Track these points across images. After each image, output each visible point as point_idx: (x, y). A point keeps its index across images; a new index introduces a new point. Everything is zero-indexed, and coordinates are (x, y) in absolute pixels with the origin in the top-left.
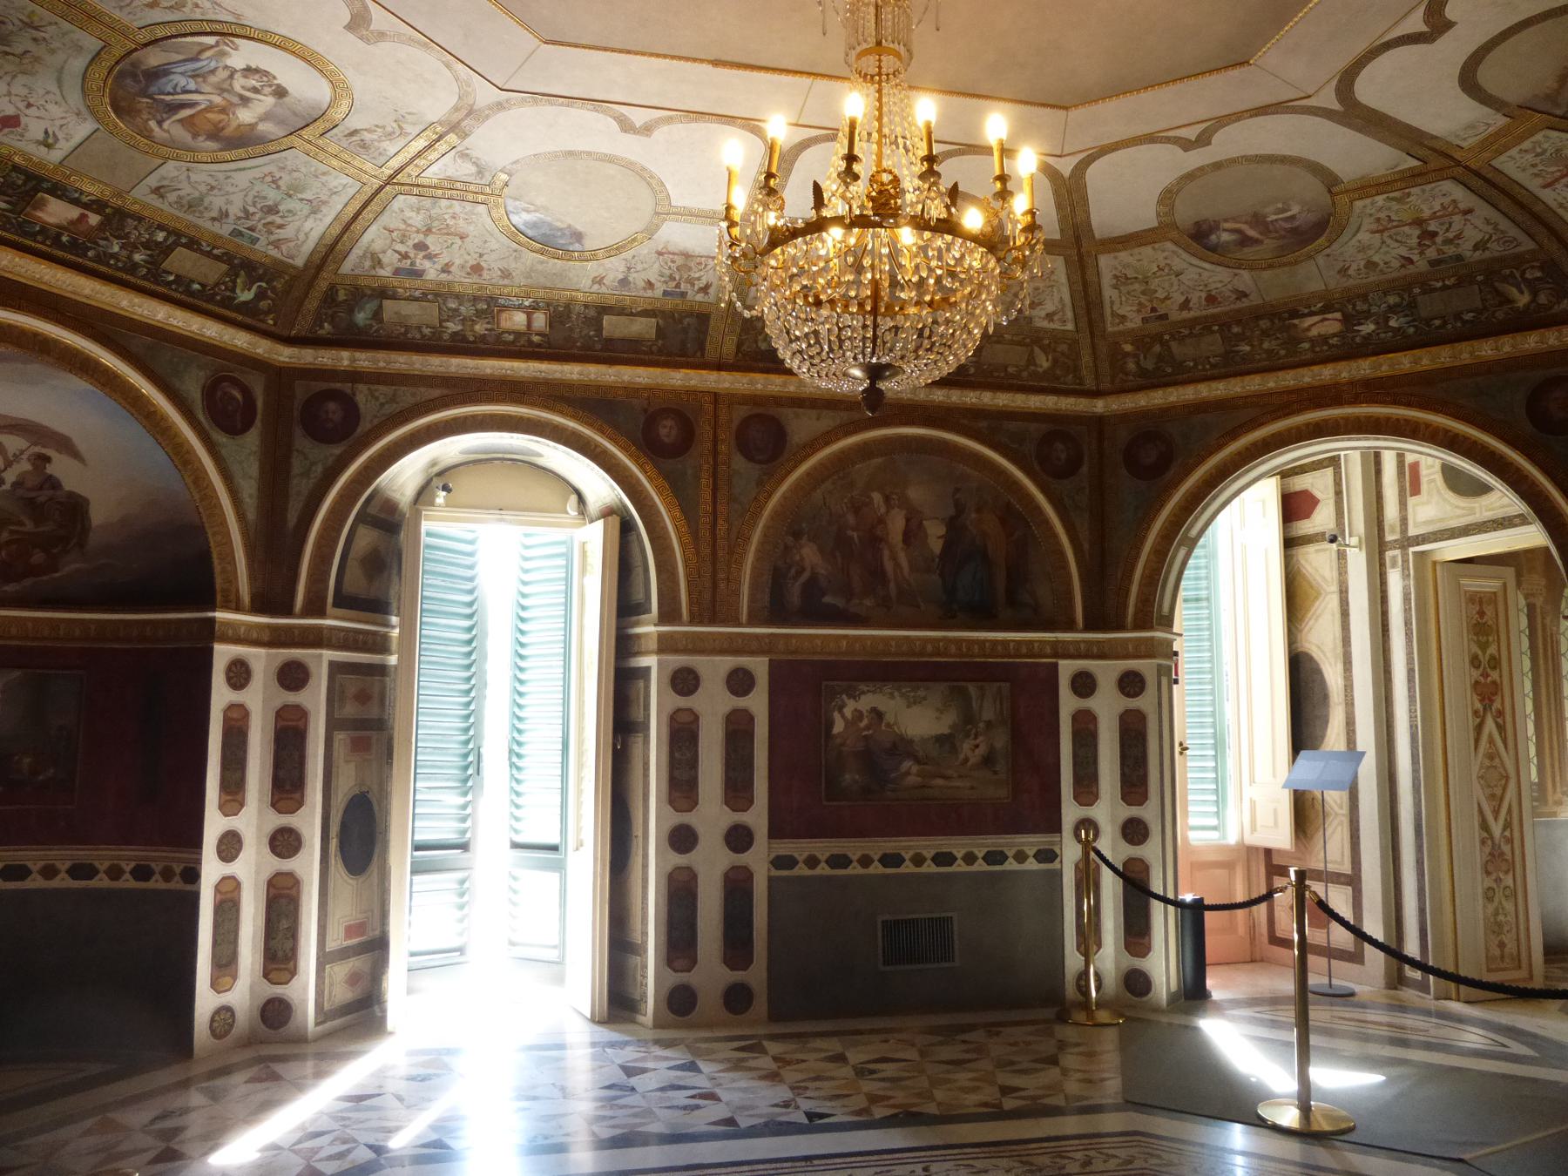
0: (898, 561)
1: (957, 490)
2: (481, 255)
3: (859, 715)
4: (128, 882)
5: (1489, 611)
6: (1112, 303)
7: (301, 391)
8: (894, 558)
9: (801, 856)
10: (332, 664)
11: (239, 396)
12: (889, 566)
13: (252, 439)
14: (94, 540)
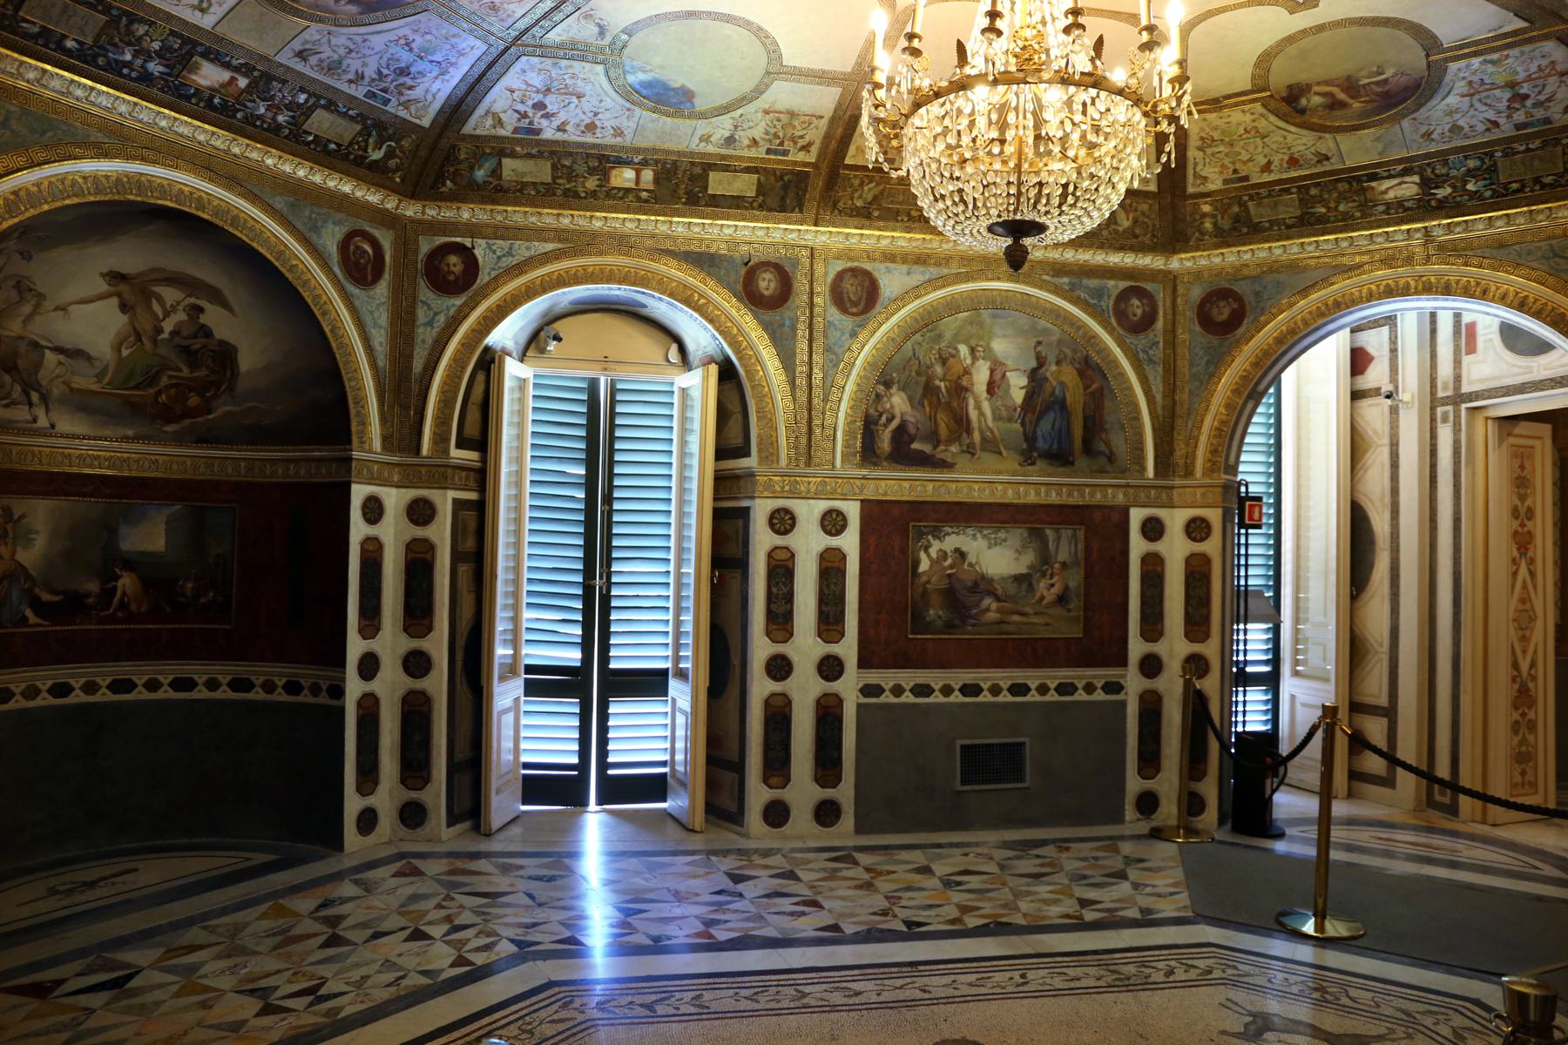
0: (980, 409)
1: (1039, 343)
2: (596, 114)
3: (943, 555)
4: (281, 696)
5: (1527, 463)
6: (1196, 164)
7: (426, 246)
8: (978, 407)
10: (455, 500)
11: (370, 250)
13: (382, 289)
14: (242, 385)
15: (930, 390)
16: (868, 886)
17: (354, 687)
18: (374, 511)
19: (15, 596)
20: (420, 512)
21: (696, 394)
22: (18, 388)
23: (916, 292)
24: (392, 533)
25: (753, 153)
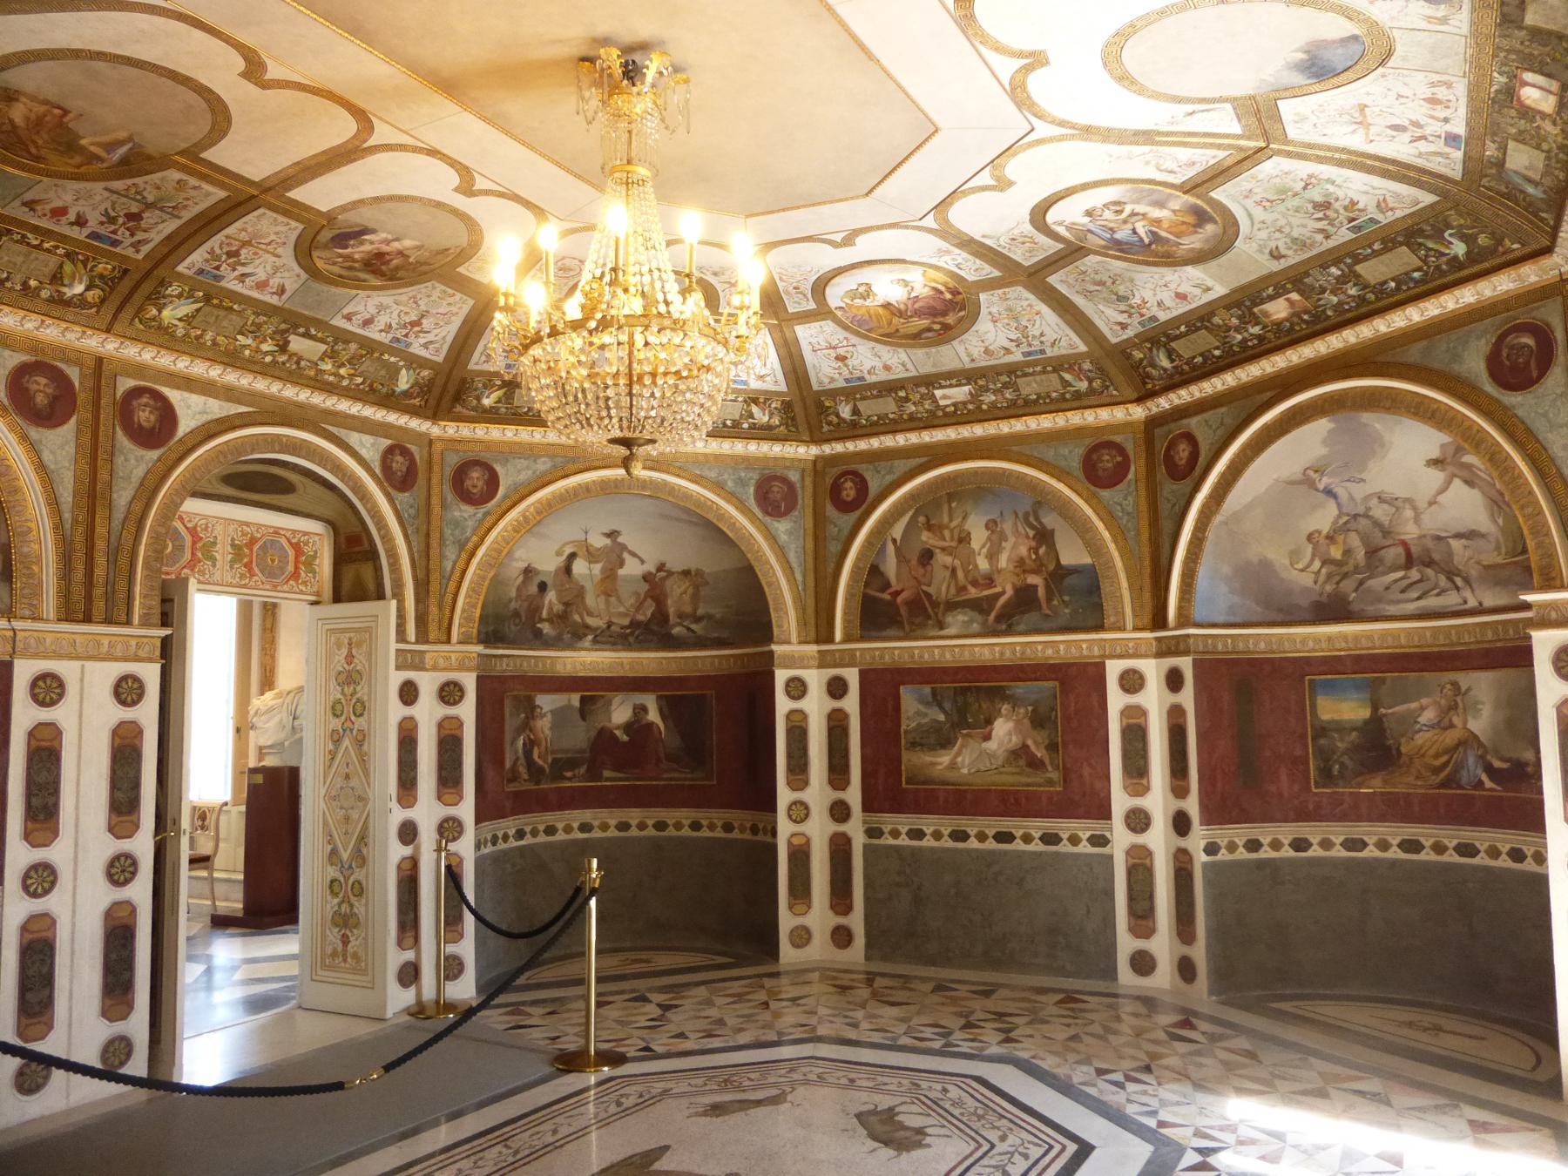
19: (1471, 760)
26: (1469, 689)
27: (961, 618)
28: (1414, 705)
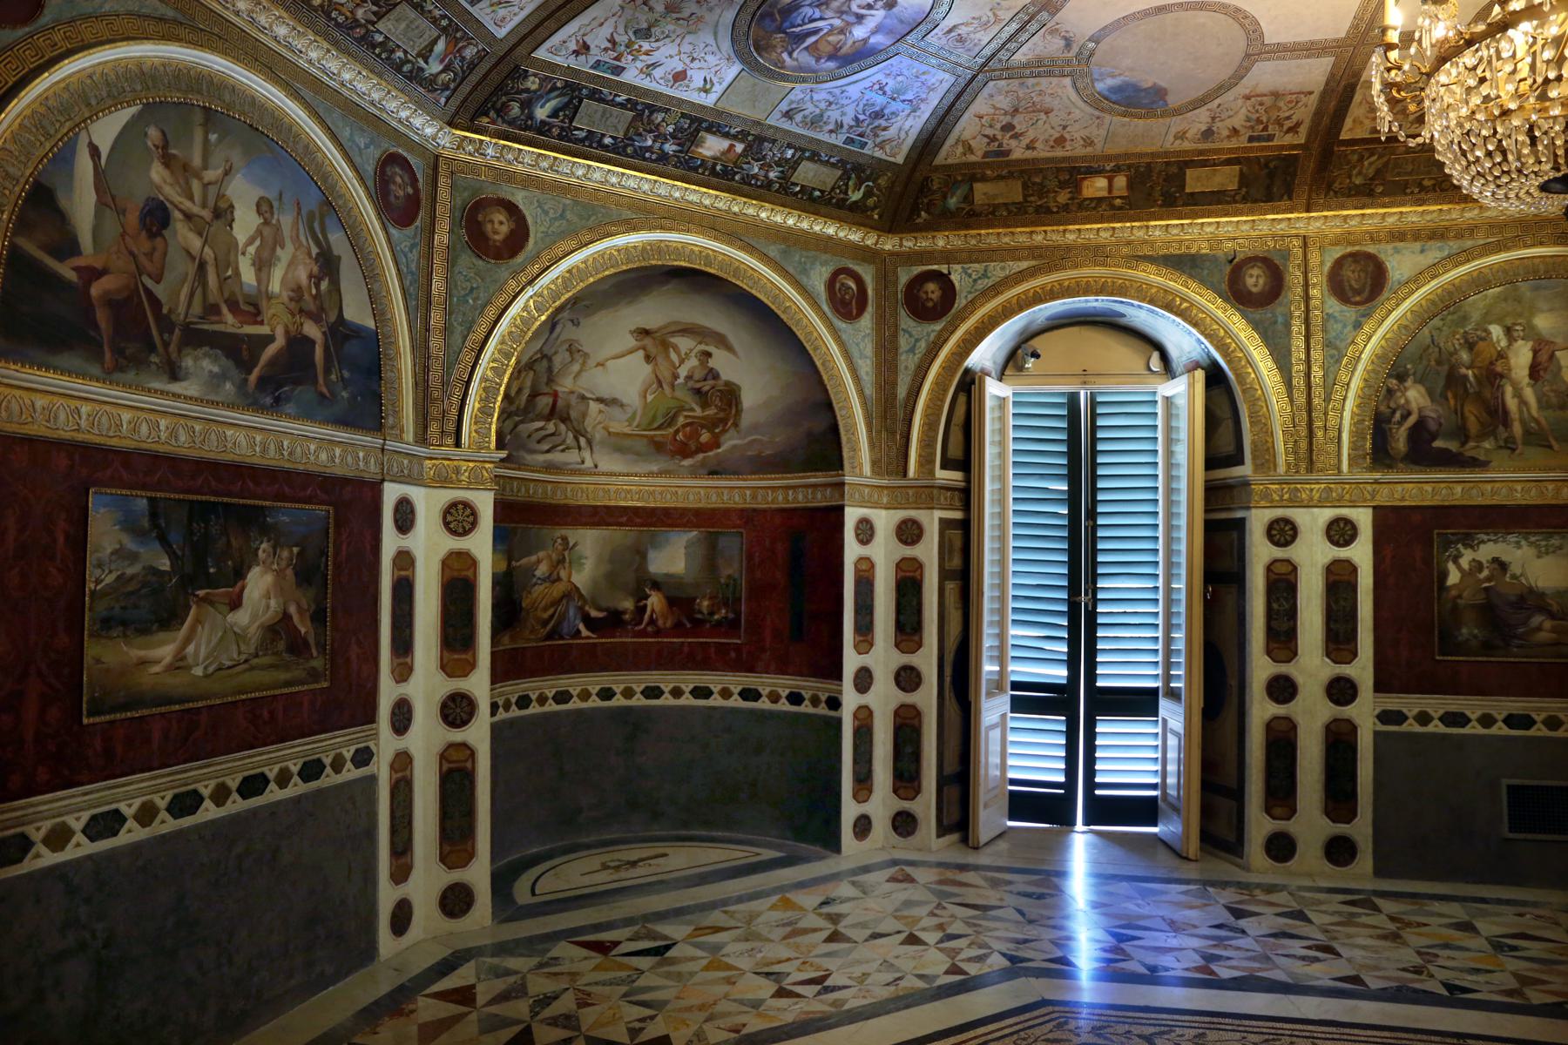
2: (1065, 127)
3: (1479, 566)
4: (784, 706)
7: (904, 276)
8: (1518, 394)
9: (1411, 712)
10: (941, 520)
11: (853, 286)
12: (1512, 403)
13: (866, 321)
14: (746, 420)
15: (1454, 380)
16: (1395, 937)
17: (851, 700)
18: (866, 532)
19: (572, 612)
20: (909, 533)
21: (1182, 402)
22: (570, 435)
23: (1432, 271)
24: (884, 554)
25: (1234, 143)
26: (575, 545)
27: (207, 365)
28: (533, 558)
